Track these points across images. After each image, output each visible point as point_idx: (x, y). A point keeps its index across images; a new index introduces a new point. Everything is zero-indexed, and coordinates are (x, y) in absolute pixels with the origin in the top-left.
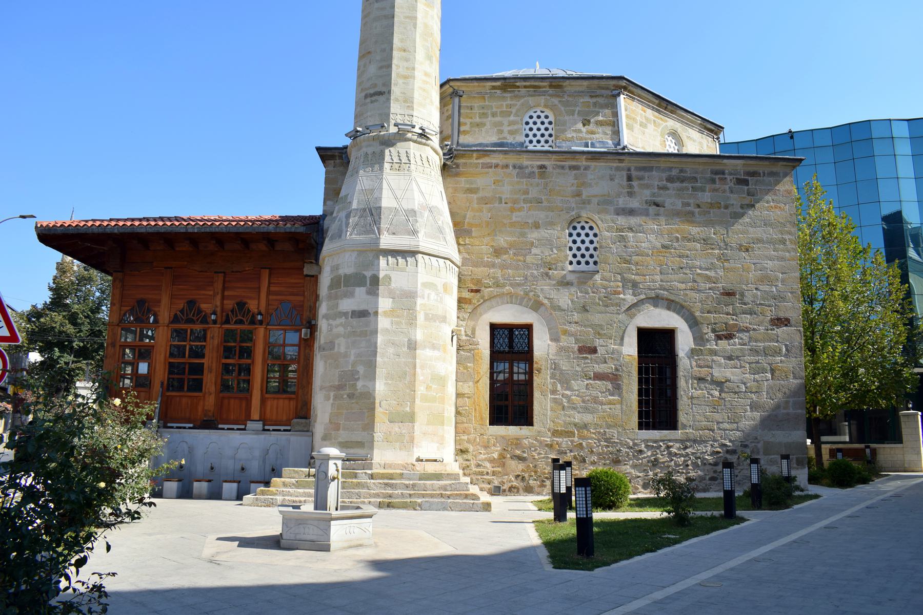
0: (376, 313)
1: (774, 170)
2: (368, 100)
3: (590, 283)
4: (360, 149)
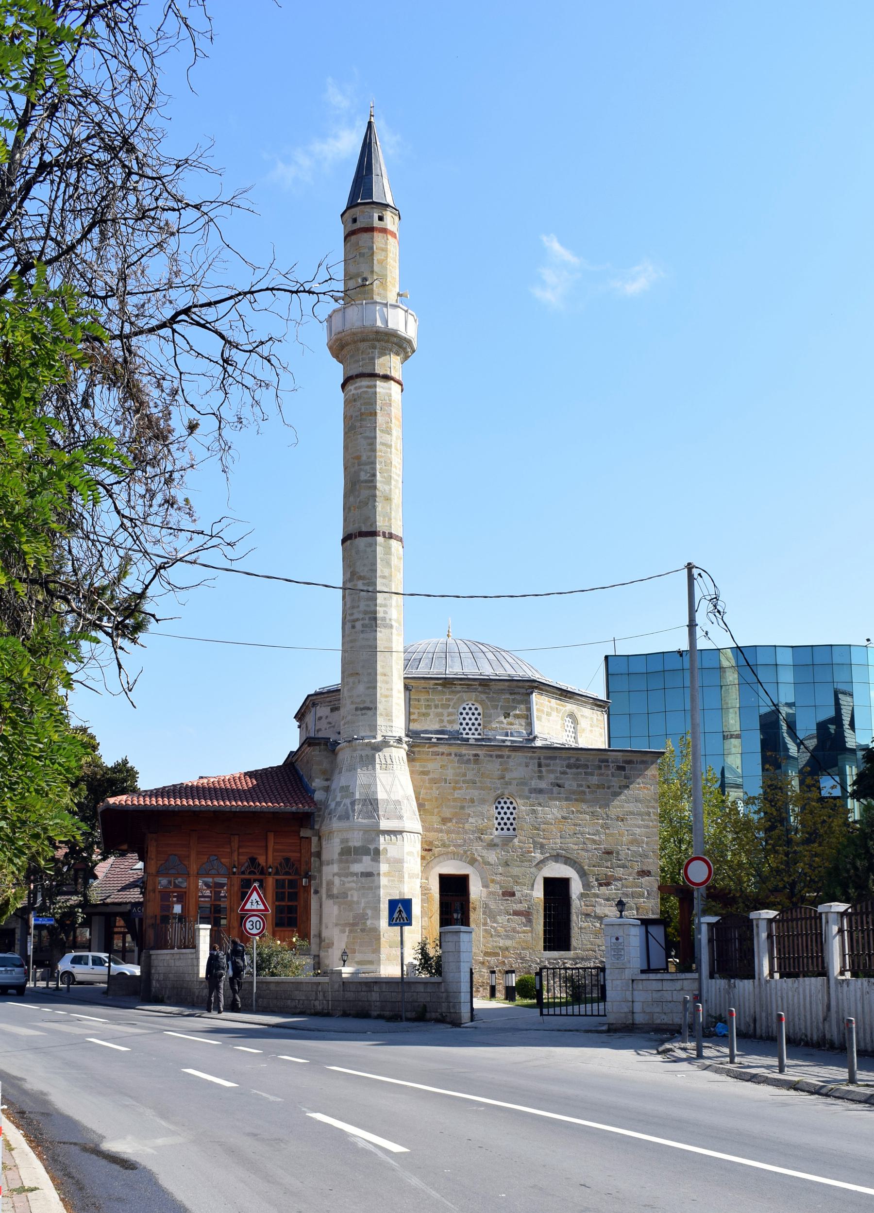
0: (379, 874)
1: (645, 759)
2: (359, 712)
3: (511, 844)
4: (355, 750)
